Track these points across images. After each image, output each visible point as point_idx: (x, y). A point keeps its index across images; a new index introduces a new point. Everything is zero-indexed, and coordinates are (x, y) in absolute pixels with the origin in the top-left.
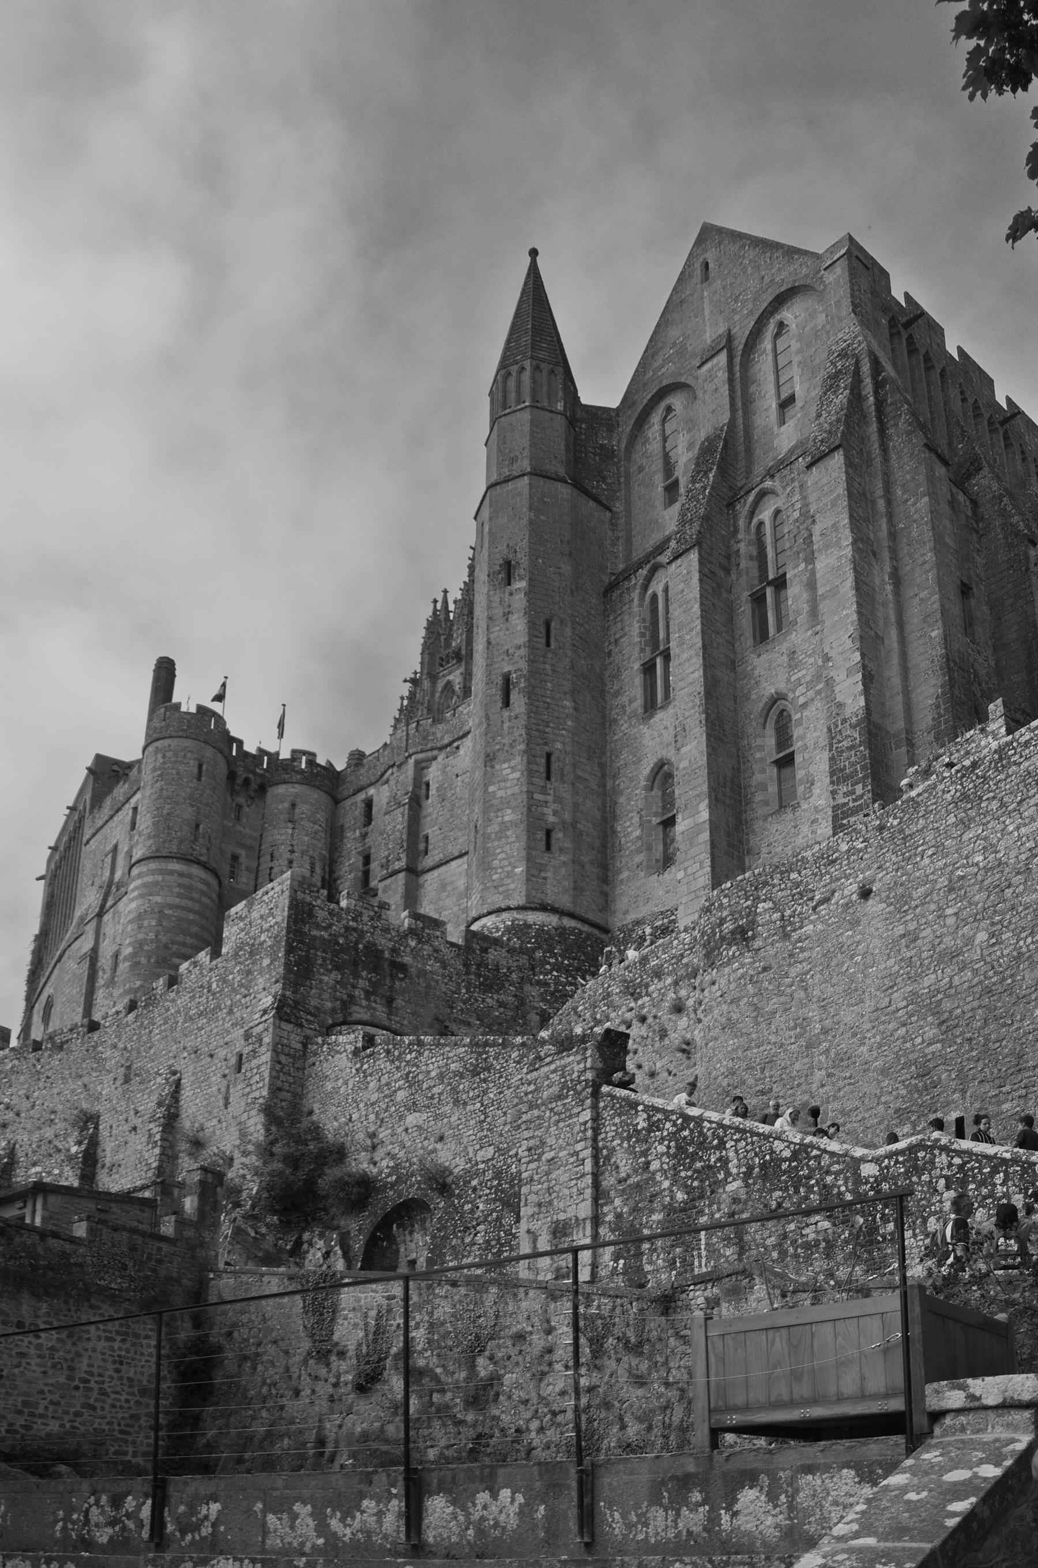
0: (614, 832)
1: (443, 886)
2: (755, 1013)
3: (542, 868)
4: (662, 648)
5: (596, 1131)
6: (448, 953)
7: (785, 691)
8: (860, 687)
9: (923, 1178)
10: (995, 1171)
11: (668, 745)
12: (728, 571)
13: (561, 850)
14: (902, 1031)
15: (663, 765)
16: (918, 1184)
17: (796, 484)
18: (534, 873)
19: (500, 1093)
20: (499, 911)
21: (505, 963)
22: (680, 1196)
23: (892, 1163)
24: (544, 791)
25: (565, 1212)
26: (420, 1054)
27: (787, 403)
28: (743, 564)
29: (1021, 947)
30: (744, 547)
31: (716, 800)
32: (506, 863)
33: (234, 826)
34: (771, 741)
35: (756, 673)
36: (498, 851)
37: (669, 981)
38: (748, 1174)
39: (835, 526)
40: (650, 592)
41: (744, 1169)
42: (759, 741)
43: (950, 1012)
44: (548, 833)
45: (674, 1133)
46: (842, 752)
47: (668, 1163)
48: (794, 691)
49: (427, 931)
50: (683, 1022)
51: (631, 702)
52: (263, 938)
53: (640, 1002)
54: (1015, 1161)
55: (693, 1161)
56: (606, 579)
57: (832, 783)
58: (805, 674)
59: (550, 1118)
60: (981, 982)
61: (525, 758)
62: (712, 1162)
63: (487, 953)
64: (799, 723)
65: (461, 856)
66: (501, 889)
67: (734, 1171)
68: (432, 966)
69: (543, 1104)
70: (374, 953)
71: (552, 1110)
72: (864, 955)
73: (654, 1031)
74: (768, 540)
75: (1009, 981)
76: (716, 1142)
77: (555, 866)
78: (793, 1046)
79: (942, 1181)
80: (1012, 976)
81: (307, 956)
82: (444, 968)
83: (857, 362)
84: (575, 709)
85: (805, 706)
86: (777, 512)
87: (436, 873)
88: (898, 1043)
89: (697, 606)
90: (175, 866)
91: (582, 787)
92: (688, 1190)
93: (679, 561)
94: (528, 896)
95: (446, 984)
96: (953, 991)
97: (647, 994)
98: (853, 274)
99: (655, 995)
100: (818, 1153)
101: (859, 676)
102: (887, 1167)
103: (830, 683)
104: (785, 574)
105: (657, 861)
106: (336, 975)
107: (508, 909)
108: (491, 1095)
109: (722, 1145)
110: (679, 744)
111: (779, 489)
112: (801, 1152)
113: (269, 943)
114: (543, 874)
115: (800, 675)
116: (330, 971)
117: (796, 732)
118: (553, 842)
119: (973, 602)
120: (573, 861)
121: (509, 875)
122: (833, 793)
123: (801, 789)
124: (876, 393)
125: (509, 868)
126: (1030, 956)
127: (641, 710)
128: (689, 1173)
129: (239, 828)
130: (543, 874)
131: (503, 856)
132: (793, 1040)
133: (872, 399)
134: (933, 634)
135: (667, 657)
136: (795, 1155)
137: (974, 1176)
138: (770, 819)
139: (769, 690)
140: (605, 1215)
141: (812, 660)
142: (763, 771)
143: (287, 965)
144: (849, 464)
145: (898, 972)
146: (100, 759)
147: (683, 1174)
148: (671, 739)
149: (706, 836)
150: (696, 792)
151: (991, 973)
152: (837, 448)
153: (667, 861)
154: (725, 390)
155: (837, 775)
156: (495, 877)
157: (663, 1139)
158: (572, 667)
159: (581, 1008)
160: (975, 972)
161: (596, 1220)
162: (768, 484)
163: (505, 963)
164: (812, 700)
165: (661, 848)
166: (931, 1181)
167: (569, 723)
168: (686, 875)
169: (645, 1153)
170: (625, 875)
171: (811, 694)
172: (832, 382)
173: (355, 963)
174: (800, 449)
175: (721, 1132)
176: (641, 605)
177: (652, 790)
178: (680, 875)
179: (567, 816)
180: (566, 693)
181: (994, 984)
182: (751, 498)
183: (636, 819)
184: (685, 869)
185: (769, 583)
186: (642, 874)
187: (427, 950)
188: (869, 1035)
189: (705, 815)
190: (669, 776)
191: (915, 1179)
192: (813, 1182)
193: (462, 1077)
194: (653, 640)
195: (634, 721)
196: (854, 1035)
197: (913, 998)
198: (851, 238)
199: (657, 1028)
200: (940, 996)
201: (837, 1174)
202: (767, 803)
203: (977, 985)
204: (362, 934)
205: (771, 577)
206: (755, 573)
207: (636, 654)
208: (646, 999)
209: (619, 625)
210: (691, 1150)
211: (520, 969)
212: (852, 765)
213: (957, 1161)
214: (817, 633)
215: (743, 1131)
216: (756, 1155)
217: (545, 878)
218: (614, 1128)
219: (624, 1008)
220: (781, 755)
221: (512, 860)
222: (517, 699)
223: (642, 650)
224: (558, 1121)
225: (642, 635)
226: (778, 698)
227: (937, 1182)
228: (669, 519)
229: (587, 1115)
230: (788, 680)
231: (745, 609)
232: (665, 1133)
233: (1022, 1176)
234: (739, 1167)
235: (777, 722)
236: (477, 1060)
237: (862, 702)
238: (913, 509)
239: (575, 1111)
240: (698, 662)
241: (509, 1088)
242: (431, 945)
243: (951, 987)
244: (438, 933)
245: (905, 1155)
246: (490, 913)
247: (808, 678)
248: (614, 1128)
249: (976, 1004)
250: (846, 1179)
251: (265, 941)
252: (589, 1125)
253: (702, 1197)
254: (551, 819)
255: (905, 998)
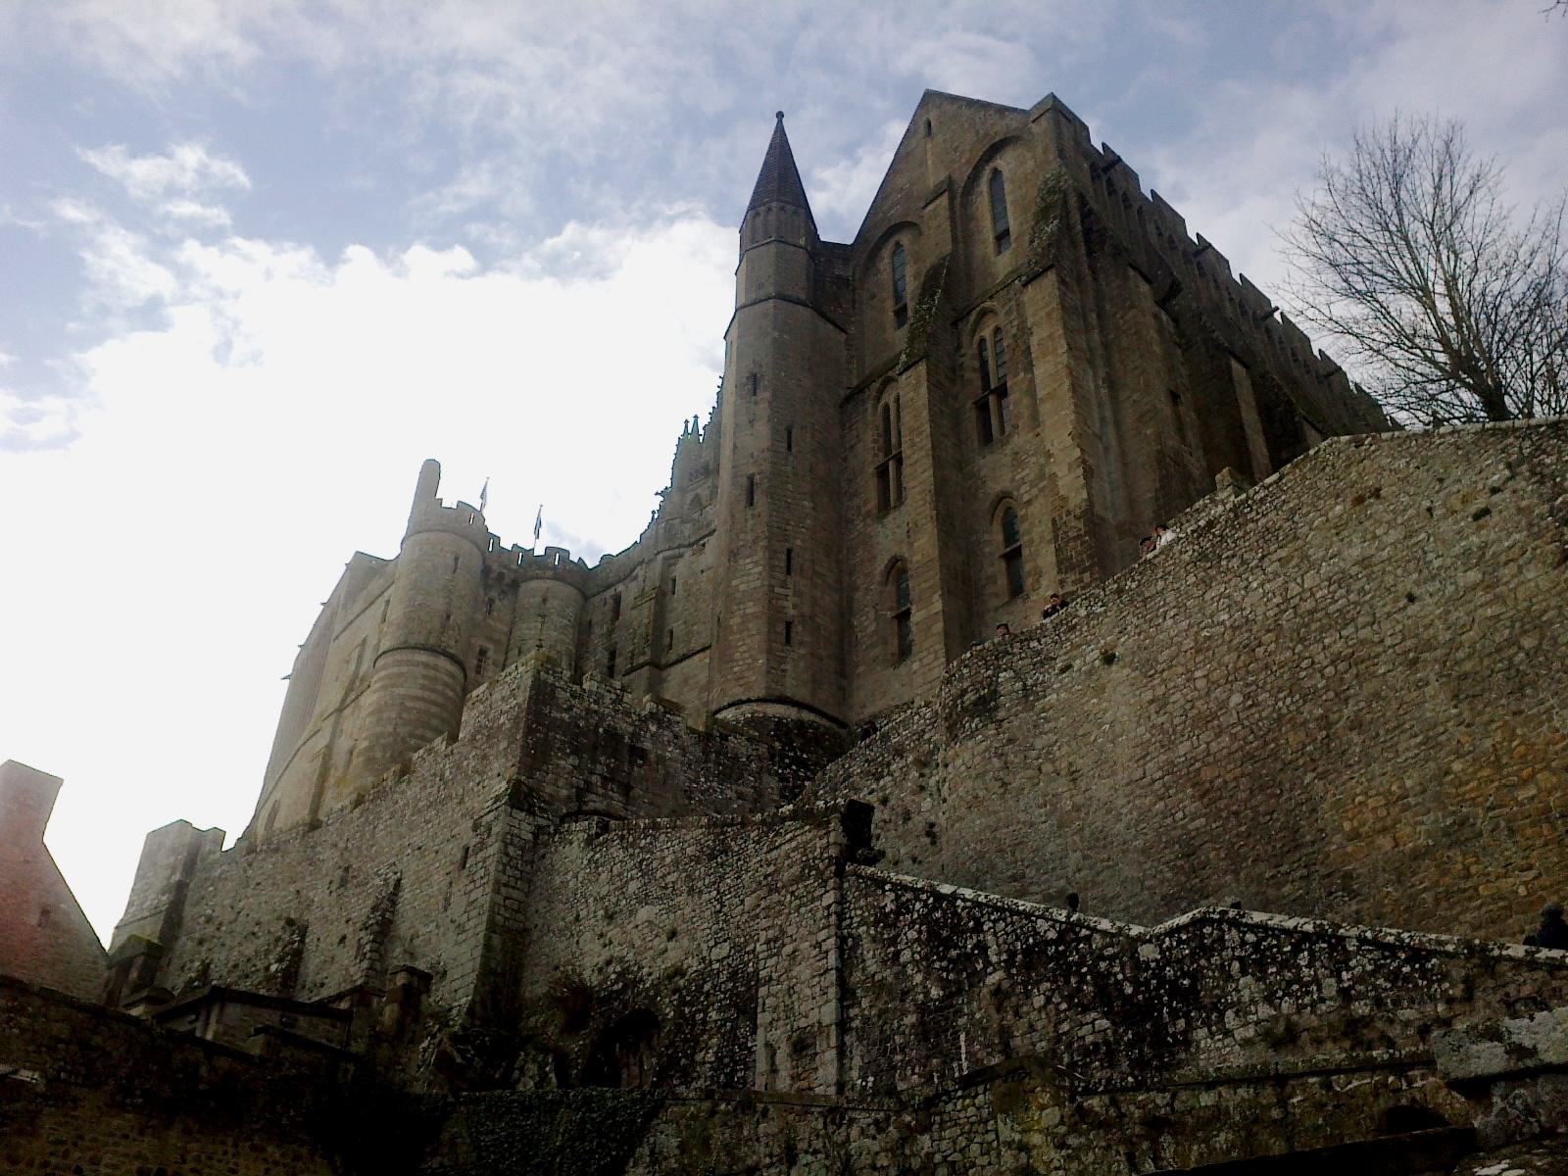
0: (851, 627)
1: (686, 681)
2: (1002, 790)
3: (782, 660)
4: (894, 453)
5: (841, 916)
6: (687, 740)
7: (1010, 489)
8: (1082, 481)
9: (1213, 960)
10: (1297, 950)
11: (901, 542)
12: (953, 381)
13: (801, 643)
14: (1160, 806)
15: (897, 561)
16: (1208, 969)
17: (1013, 303)
18: (775, 666)
19: (737, 878)
20: (741, 702)
21: (744, 750)
22: (935, 992)
23: (1175, 944)
24: (784, 585)
25: (806, 1017)
26: (656, 839)
27: (1002, 237)
28: (968, 375)
29: (1280, 709)
30: (970, 361)
31: (948, 593)
32: (747, 655)
33: (485, 619)
34: (1000, 537)
35: (982, 474)
36: (740, 643)
37: (911, 758)
38: (1010, 963)
39: (1051, 337)
40: (882, 402)
41: (1004, 957)
42: (986, 537)
43: (1211, 782)
44: (789, 625)
45: (925, 916)
46: (1068, 542)
47: (919, 953)
48: (1018, 490)
49: (668, 716)
50: (927, 804)
51: (866, 502)
52: (502, 720)
53: (882, 783)
54: (1320, 935)
55: (947, 949)
56: (843, 393)
57: (1060, 571)
58: (1029, 473)
59: (791, 902)
60: (1241, 748)
61: (767, 553)
62: (969, 950)
63: (727, 740)
64: (1025, 518)
65: (703, 650)
66: (742, 682)
67: (994, 959)
68: (672, 752)
69: (783, 887)
70: (613, 735)
71: (792, 893)
72: (1112, 724)
73: (897, 814)
74: (989, 354)
75: (1272, 745)
76: (972, 923)
77: (793, 659)
78: (1044, 826)
79: (1236, 965)
80: (1274, 740)
81: (546, 738)
82: (684, 756)
83: (1065, 196)
84: (813, 509)
85: (1029, 502)
86: (997, 330)
87: (679, 667)
88: (1157, 819)
89: (925, 413)
90: (422, 657)
91: (820, 582)
92: (944, 984)
93: (908, 373)
94: (768, 688)
95: (685, 772)
96: (1211, 759)
97: (890, 774)
98: (1057, 123)
99: (896, 775)
100: (1088, 932)
101: (1080, 471)
102: (1169, 949)
103: (1053, 476)
104: (1006, 383)
105: (893, 654)
106: (573, 760)
107: (749, 701)
108: (729, 881)
109: (978, 928)
110: (911, 540)
111: (998, 308)
112: (1068, 933)
113: (508, 726)
114: (783, 667)
115: (1024, 474)
116: (569, 755)
117: (1023, 528)
118: (793, 634)
119: (1182, 408)
120: (812, 654)
121: (750, 667)
122: (1062, 583)
123: (1029, 582)
124: (1082, 222)
125: (750, 661)
126: (1291, 719)
127: (875, 511)
128: (945, 964)
129: (489, 621)
130: (783, 667)
131: (744, 648)
132: (1043, 819)
133: (1079, 227)
134: (1148, 432)
135: (899, 461)
136: (1061, 938)
137: (1274, 957)
138: (1001, 610)
139: (994, 488)
140: (852, 1019)
141: (1034, 459)
142: (992, 565)
143: (525, 747)
144: (1062, 282)
145: (1150, 740)
146: (357, 552)
147: (937, 965)
148: (905, 536)
149: (939, 627)
150: (928, 585)
151: (1251, 738)
152: (1050, 268)
153: (904, 652)
154: (947, 226)
155: (1063, 565)
156: (736, 669)
157: (913, 922)
158: (811, 471)
159: (821, 792)
160: (1234, 737)
161: (843, 1025)
162: (988, 304)
163: (744, 750)
164: (1036, 496)
165: (896, 642)
166: (1222, 965)
167: (809, 522)
168: (922, 666)
169: (893, 941)
170: (861, 669)
171: (1035, 491)
172: (1044, 214)
173: (595, 748)
174: (1015, 274)
175: (976, 912)
176: (875, 415)
177: (886, 583)
178: (915, 666)
179: (806, 609)
180: (805, 494)
181: (1257, 749)
182: (973, 317)
183: (872, 615)
184: (921, 660)
185: (992, 392)
186: (879, 668)
187: (667, 735)
188: (1125, 811)
189: (938, 606)
190: (904, 571)
191: (1203, 962)
192: (1084, 970)
193: (697, 863)
194: (887, 448)
195: (869, 521)
196: (1109, 812)
197: (1170, 768)
198: (1054, 97)
199: (899, 810)
200: (1198, 765)
201: (1112, 958)
202: (997, 595)
203: (1237, 751)
204: (602, 718)
205: (992, 387)
206: (978, 383)
207: (870, 457)
208: (888, 779)
209: (854, 433)
210: (945, 933)
211: (760, 759)
212: (1079, 554)
213: (1250, 937)
214: (1037, 435)
215: (1002, 910)
216: (1018, 939)
217: (783, 671)
218: (859, 912)
219: (866, 791)
220: (1008, 549)
221: (754, 652)
222: (759, 498)
223: (875, 455)
224: (800, 906)
225: (875, 441)
226: (1004, 496)
227: (1230, 965)
228: (899, 337)
229: (830, 898)
230: (1013, 480)
231: (971, 416)
232: (916, 916)
233: (1330, 954)
234: (999, 954)
235: (1003, 519)
236: (714, 841)
237: (1085, 495)
238: (1121, 322)
239: (817, 894)
240: (929, 461)
241: (747, 871)
242: (672, 731)
243: (1208, 755)
244: (679, 719)
245: (1188, 932)
246: (730, 705)
247: (1032, 476)
248: (859, 912)
249: (1238, 771)
250: (1123, 966)
251: (504, 723)
252: (832, 909)
253: (960, 992)
254: (792, 612)
255: (1161, 768)
